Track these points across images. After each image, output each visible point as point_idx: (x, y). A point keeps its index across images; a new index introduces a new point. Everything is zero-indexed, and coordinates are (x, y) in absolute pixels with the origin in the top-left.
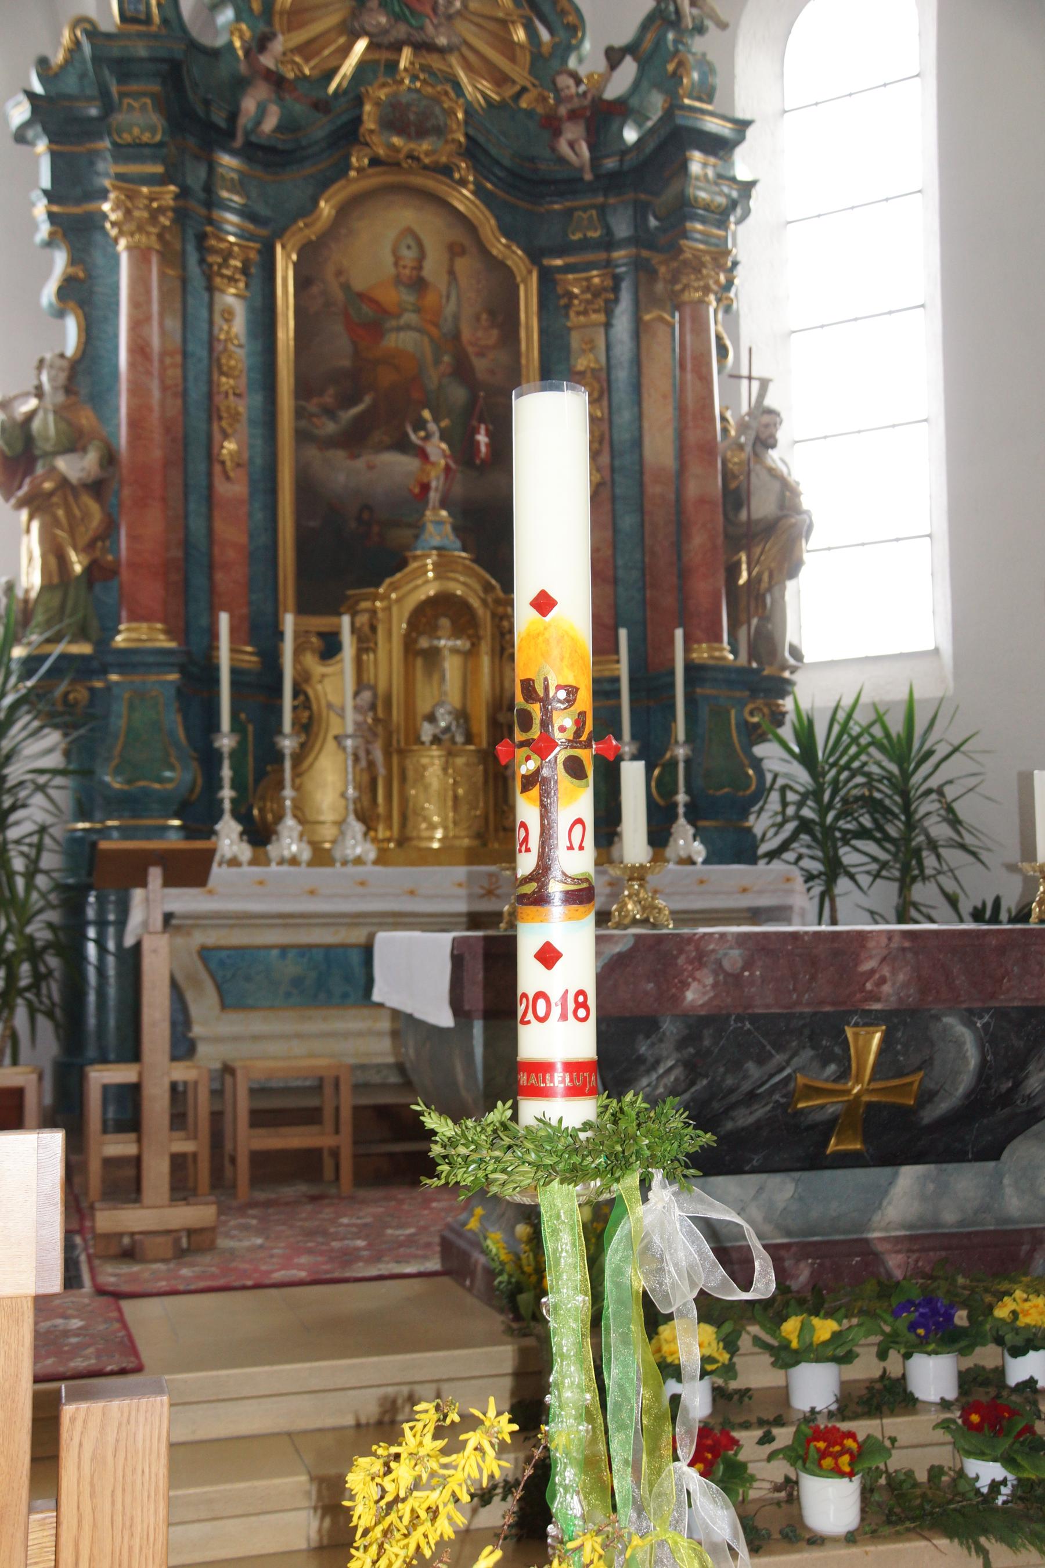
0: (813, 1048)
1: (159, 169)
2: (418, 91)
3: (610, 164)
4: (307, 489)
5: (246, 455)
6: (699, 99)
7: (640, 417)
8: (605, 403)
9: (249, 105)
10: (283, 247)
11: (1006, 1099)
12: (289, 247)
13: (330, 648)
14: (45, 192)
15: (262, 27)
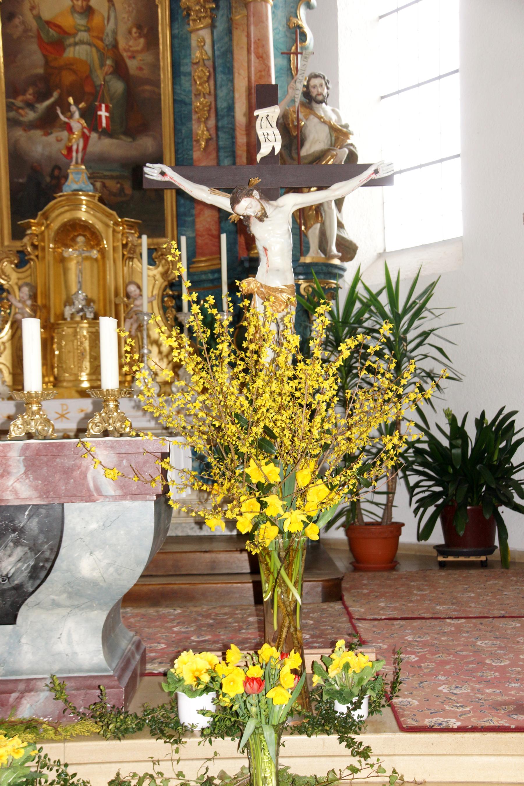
8: (212, 82)
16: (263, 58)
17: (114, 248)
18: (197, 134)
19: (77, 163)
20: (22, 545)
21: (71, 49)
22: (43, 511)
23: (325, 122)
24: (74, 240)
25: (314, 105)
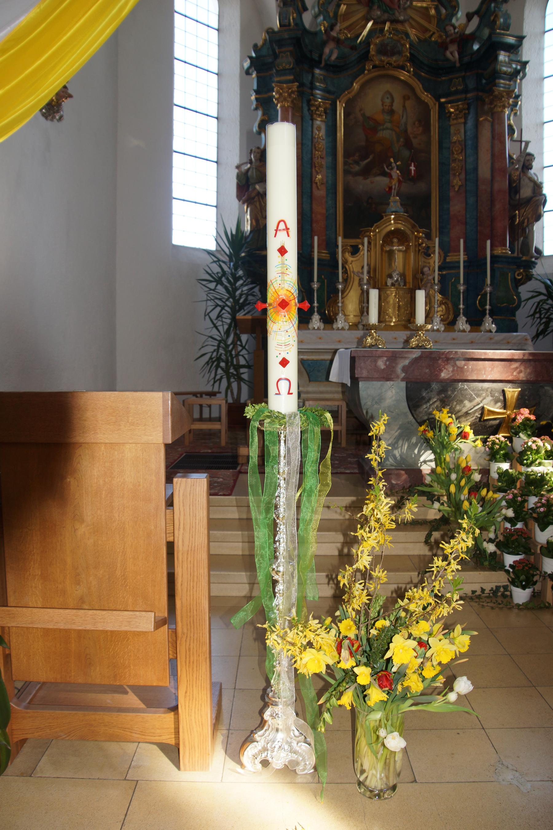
0: (492, 396)
1: (291, 77)
2: (392, 38)
3: (466, 59)
4: (347, 191)
5: (325, 180)
7: (477, 159)
8: (463, 154)
9: (327, 50)
10: (340, 102)
12: (342, 101)
13: (355, 250)
14: (255, 91)
15: (333, 21)
17: (415, 246)
19: (394, 196)
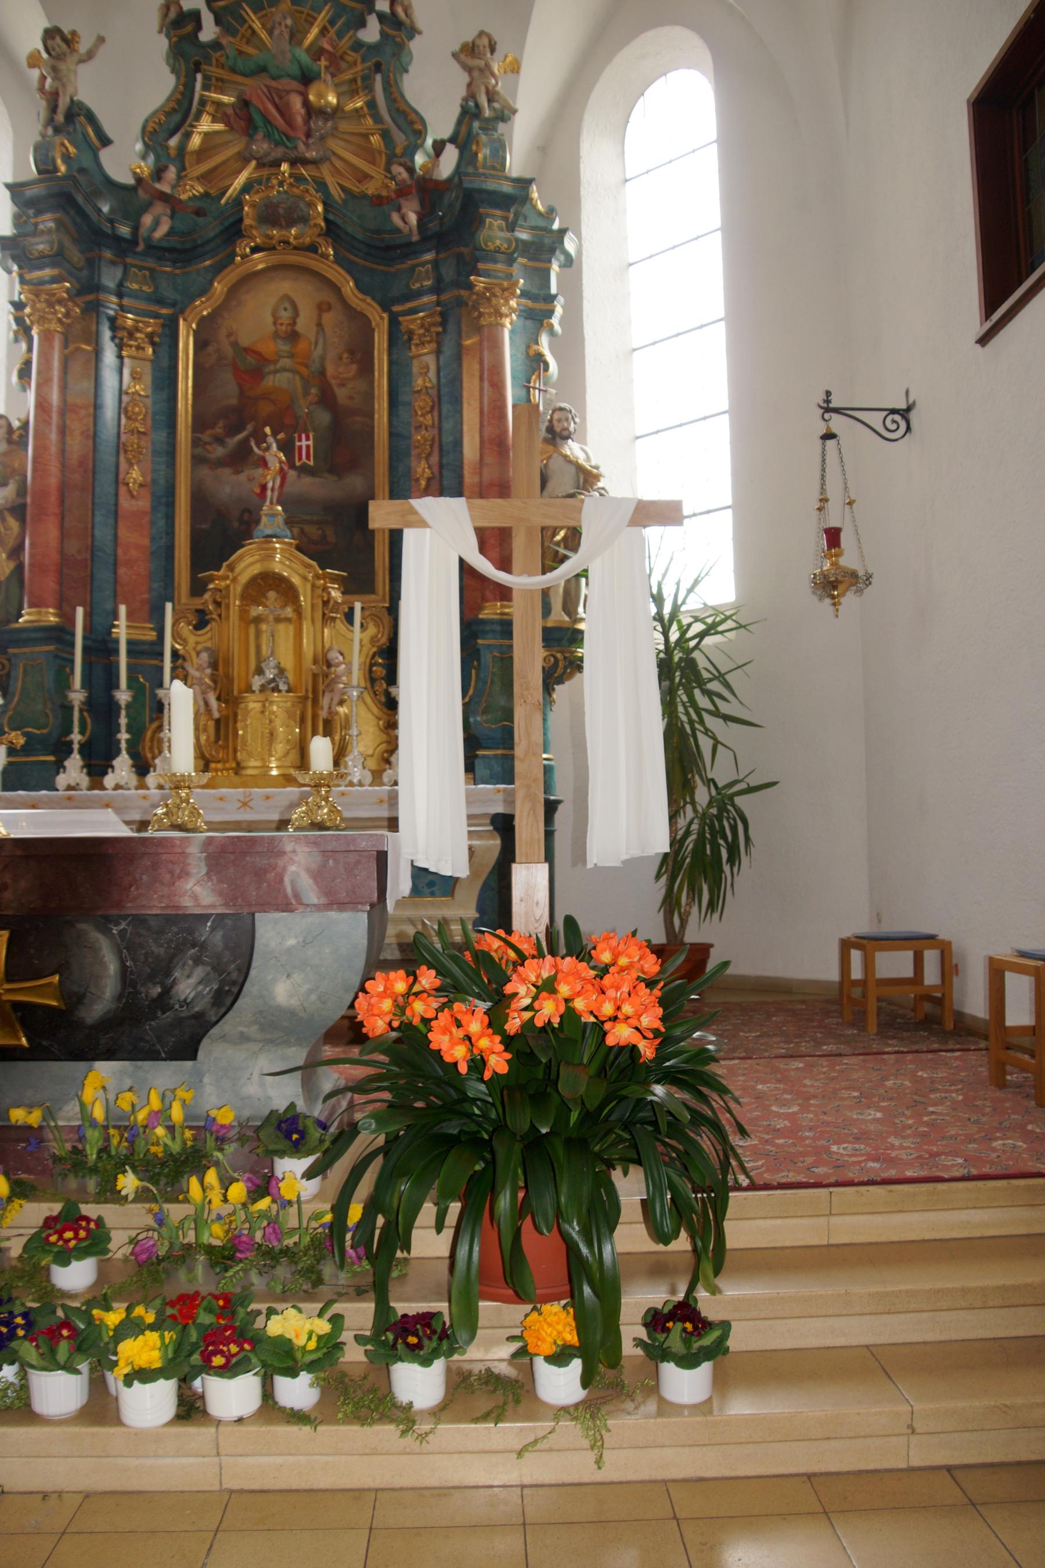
2: (286, 192)
3: (434, 226)
4: (199, 500)
5: (149, 478)
6: (494, 168)
8: (436, 414)
9: (147, 220)
10: (185, 320)
11: (163, 1002)
12: (189, 319)
16: (498, 386)
17: (313, 605)
18: (416, 472)
19: (271, 503)
20: (204, 965)
21: (272, 377)
22: (229, 922)
23: (570, 462)
24: (264, 595)
25: (558, 440)
